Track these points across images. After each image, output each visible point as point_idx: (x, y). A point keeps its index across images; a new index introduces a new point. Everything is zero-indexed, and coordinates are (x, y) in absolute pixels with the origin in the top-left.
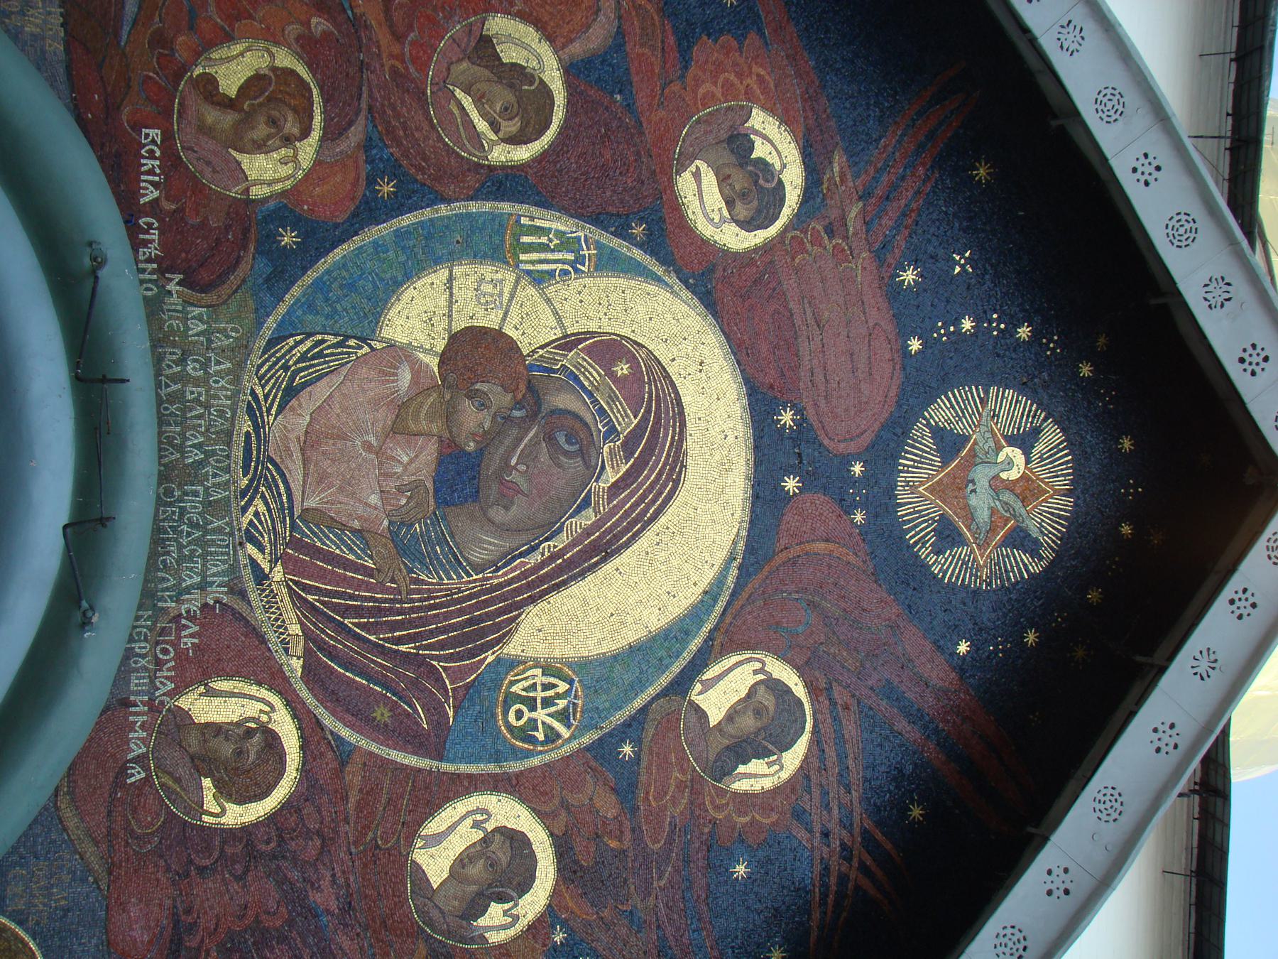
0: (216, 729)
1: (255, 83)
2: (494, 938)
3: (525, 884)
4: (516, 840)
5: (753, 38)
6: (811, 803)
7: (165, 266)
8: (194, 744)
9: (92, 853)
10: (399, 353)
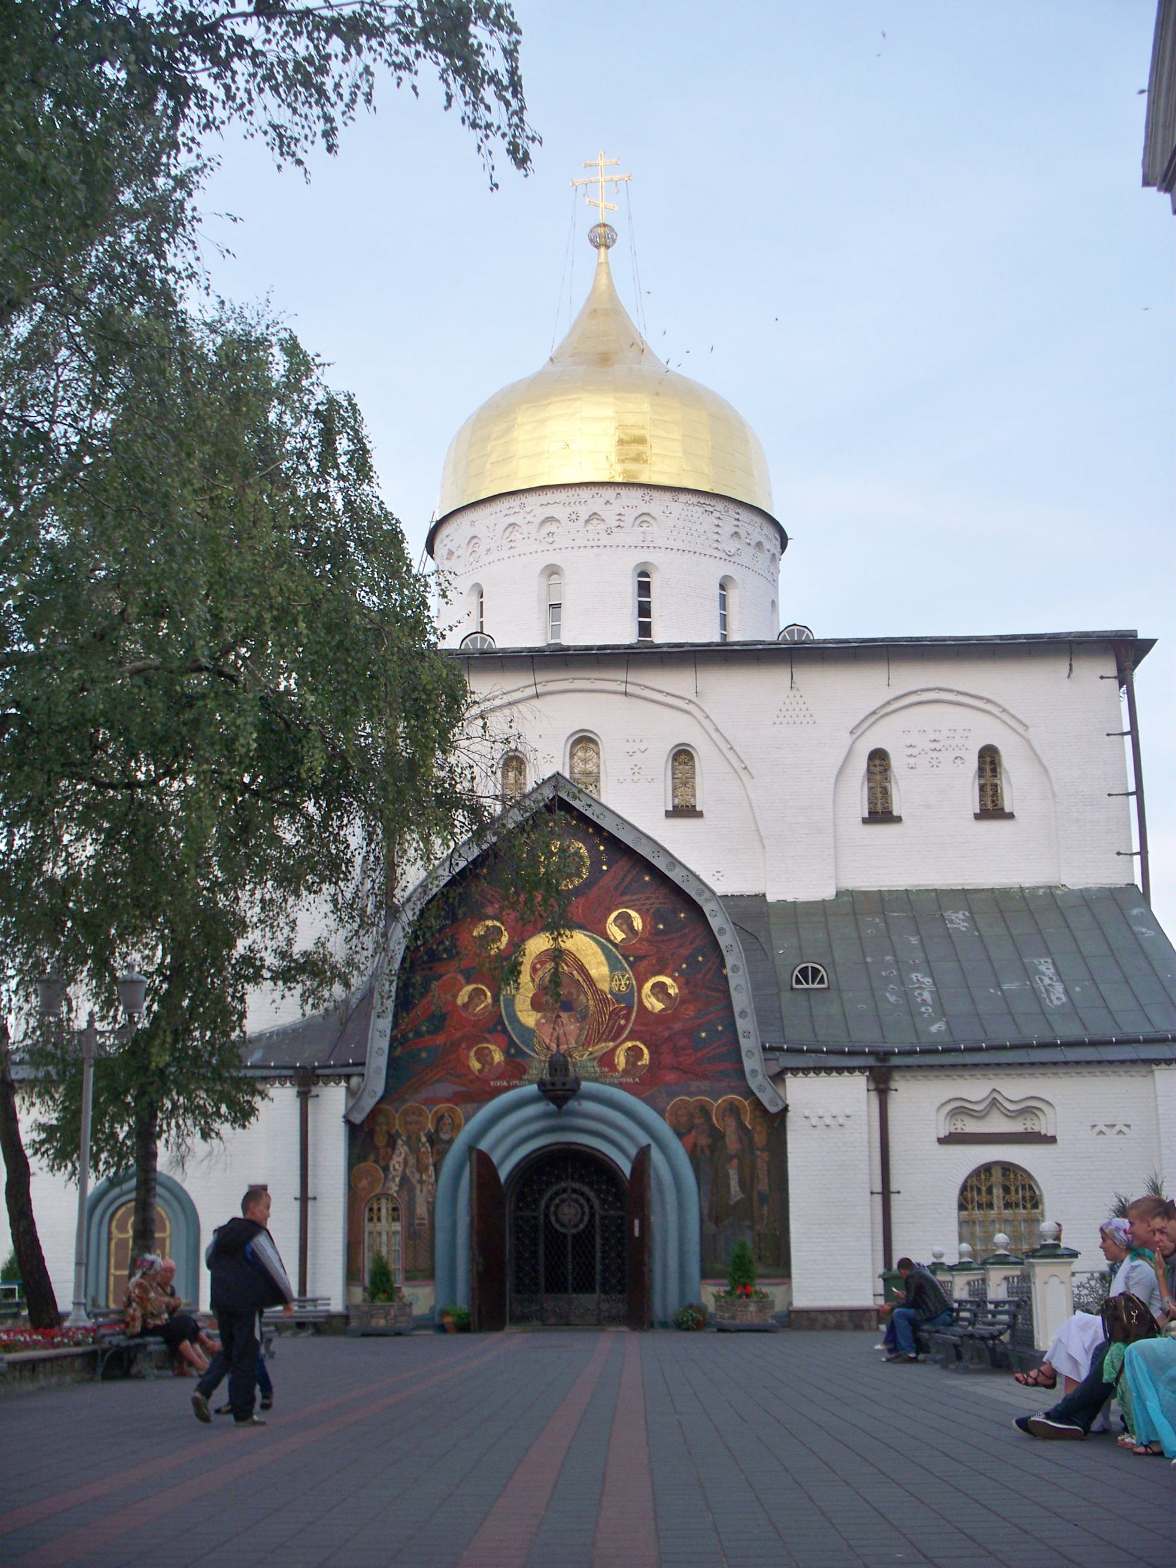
1: (479, 1060)
3: (664, 984)
4: (654, 986)
7: (521, 1079)
10: (538, 1023)
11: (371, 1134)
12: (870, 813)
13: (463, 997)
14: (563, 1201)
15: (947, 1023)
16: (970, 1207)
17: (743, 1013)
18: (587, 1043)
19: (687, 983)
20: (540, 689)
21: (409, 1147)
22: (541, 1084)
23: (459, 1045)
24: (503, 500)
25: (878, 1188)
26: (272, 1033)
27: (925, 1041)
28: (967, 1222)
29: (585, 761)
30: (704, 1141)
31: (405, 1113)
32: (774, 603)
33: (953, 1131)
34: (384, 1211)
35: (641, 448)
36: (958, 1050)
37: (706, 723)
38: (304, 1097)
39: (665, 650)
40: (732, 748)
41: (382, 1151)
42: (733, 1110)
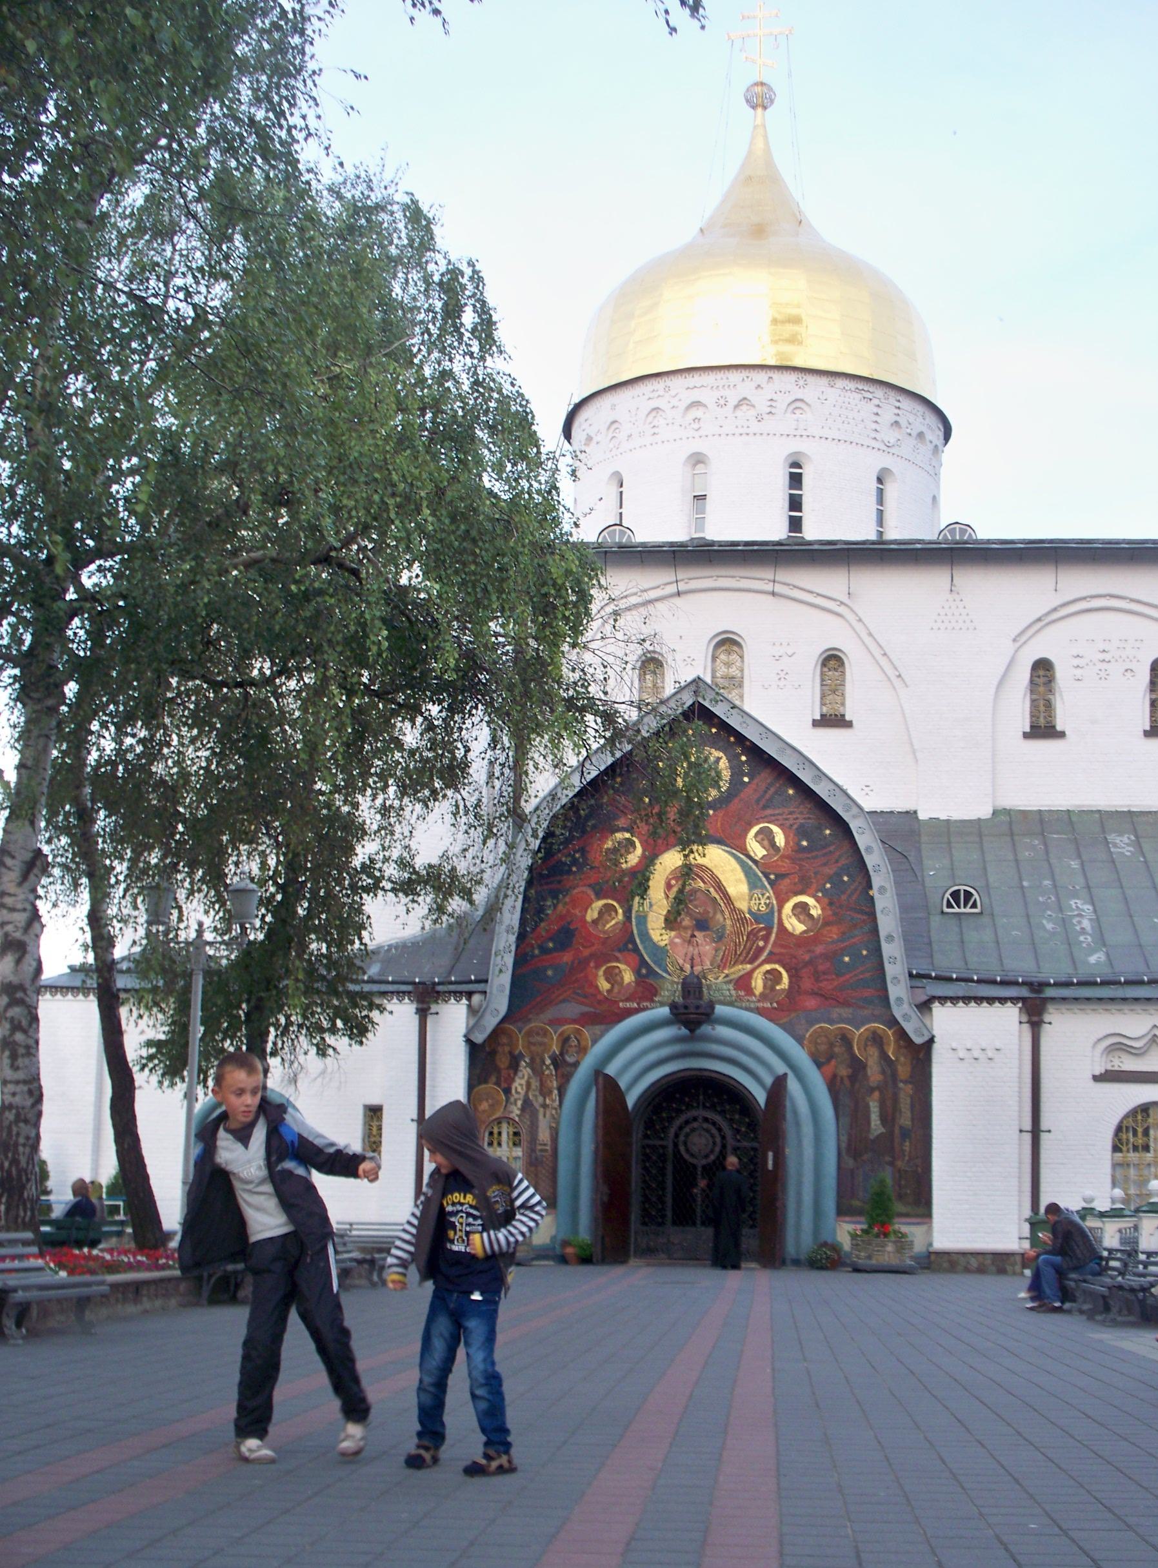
0: (765, 986)
1: (607, 980)
2: (820, 912)
4: (796, 906)
5: (588, 849)
6: (788, 823)
7: (652, 1001)
8: (768, 991)
9: (793, 1015)
10: (672, 942)
11: (493, 1053)
12: (1032, 727)
13: (592, 914)
14: (693, 1130)
15: (1107, 955)
16: (1124, 1149)
17: (890, 938)
18: (722, 966)
19: (831, 903)
20: (682, 587)
21: (533, 1069)
22: (673, 1007)
23: (588, 964)
24: (646, 382)
25: (1027, 1125)
26: (390, 946)
27: (1083, 974)
28: (1121, 1165)
29: (728, 665)
30: (844, 1072)
31: (529, 1034)
32: (934, 498)
33: (1110, 1068)
34: (504, 1136)
35: (796, 328)
36: (1118, 983)
37: (859, 627)
38: (423, 1014)
39: (816, 547)
40: (885, 654)
41: (504, 1073)
42: (876, 1039)
